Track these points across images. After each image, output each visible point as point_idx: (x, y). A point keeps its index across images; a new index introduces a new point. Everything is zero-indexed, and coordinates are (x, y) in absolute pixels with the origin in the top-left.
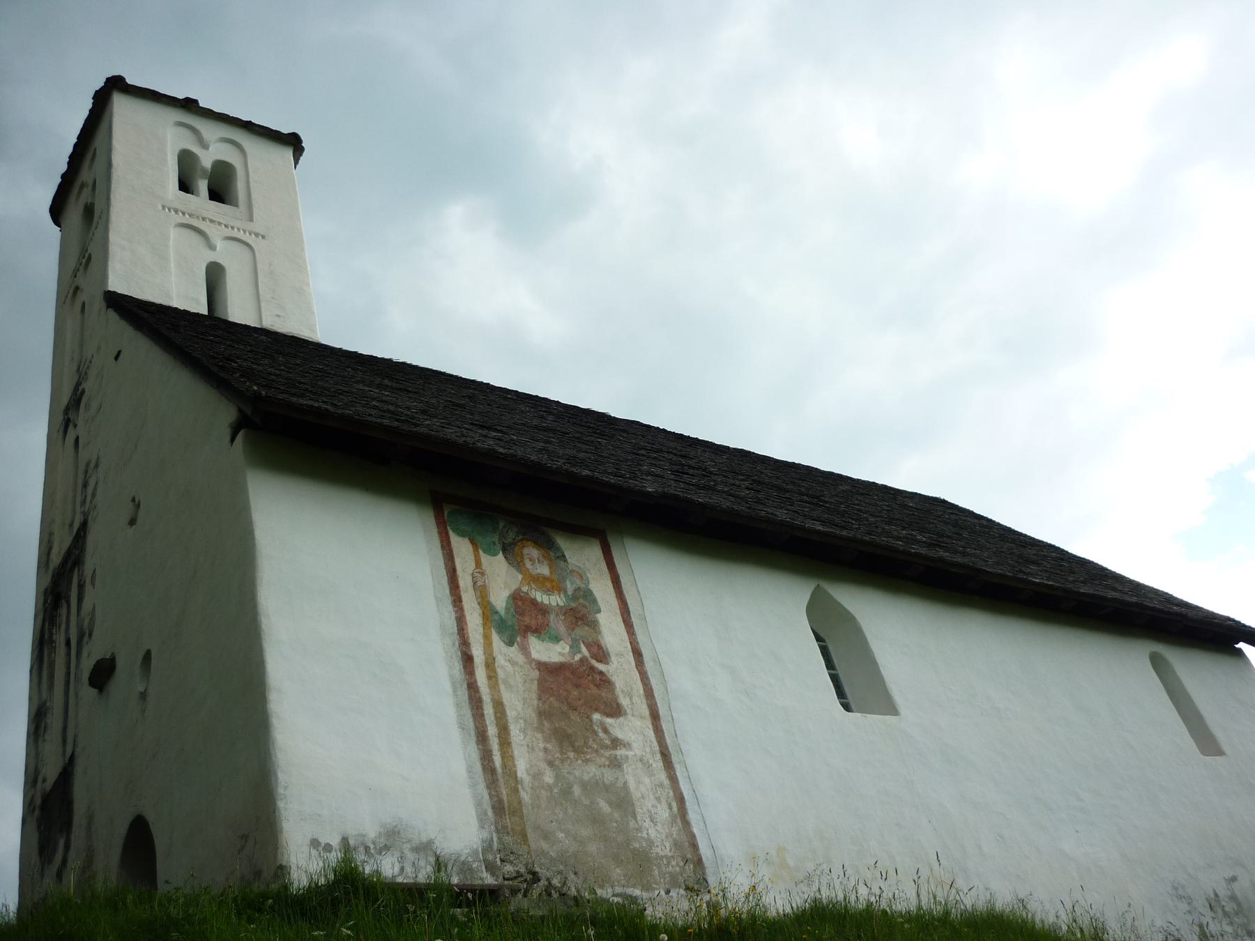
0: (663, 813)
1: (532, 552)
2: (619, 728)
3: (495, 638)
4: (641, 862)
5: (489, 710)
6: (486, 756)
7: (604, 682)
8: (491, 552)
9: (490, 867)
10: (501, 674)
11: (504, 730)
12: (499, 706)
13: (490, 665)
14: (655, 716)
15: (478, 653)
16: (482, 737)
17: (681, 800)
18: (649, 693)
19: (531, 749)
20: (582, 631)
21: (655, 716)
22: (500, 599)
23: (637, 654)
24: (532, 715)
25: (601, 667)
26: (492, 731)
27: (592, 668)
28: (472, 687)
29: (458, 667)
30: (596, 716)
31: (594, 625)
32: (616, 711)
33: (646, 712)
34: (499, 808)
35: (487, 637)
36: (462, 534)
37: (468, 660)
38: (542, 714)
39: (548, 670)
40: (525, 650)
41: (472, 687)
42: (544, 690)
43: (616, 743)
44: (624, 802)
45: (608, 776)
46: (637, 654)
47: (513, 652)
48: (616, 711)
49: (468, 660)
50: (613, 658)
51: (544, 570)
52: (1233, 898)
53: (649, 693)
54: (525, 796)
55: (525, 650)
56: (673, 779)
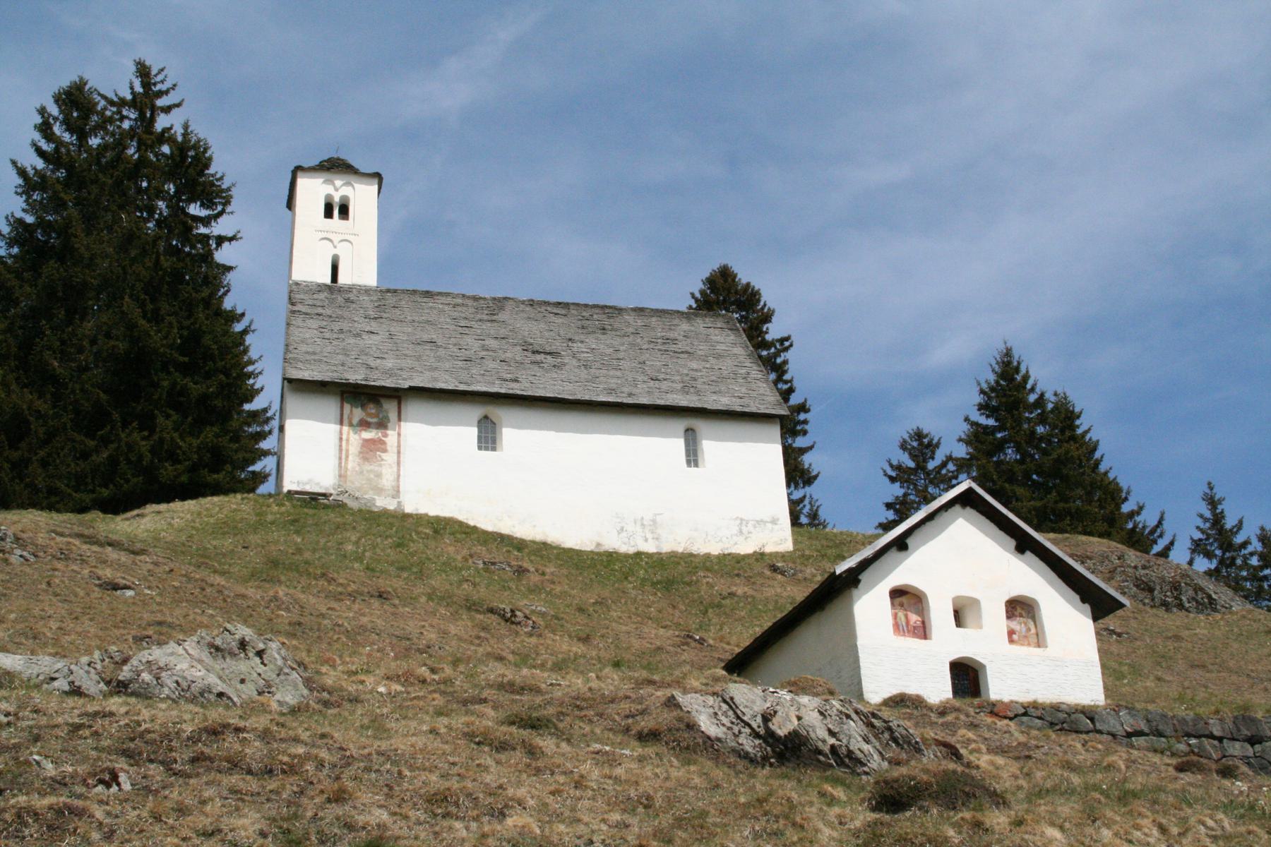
0: (392, 478)
1: (372, 406)
3: (351, 432)
4: (380, 491)
5: (344, 452)
6: (340, 464)
7: (384, 443)
8: (357, 407)
9: (334, 489)
11: (347, 457)
12: (347, 451)
13: (348, 440)
14: (399, 452)
15: (344, 437)
16: (340, 458)
17: (399, 476)
18: (399, 446)
21: (399, 452)
24: (357, 452)
26: (344, 456)
28: (341, 446)
29: (337, 441)
32: (385, 451)
34: (340, 476)
35: (348, 434)
37: (341, 439)
38: (360, 453)
39: (366, 441)
40: (360, 435)
41: (341, 446)
42: (363, 446)
44: (379, 475)
45: (376, 468)
47: (356, 437)
48: (385, 451)
51: (373, 411)
52: (654, 521)
53: (399, 446)
54: (349, 473)
55: (360, 435)
56: (399, 470)
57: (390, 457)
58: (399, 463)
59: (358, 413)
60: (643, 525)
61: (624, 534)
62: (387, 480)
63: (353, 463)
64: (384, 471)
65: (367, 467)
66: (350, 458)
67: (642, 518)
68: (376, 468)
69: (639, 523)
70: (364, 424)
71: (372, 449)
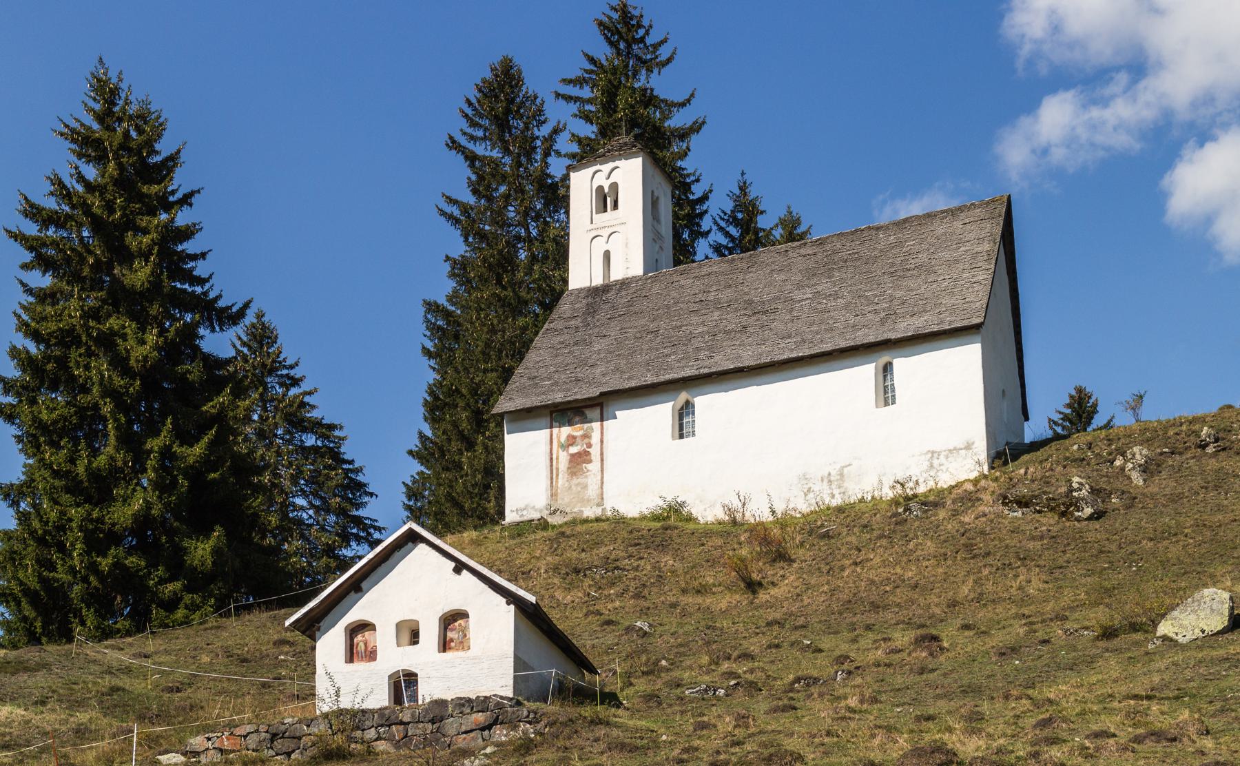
2: (589, 466)
6: (552, 483)
8: (564, 425)
10: (560, 460)
11: (557, 475)
12: (557, 469)
13: (557, 459)
14: (602, 460)
15: (554, 457)
16: (552, 478)
18: (602, 454)
19: (563, 478)
20: (586, 440)
21: (602, 460)
22: (563, 439)
23: (602, 442)
24: (565, 469)
25: (588, 450)
26: (554, 476)
27: (586, 451)
28: (552, 466)
29: (548, 461)
30: (584, 465)
32: (590, 461)
33: (599, 459)
35: (558, 451)
36: (556, 422)
37: (551, 459)
38: (568, 468)
39: (572, 456)
40: (567, 451)
41: (552, 466)
42: (570, 461)
43: (588, 471)
46: (602, 442)
47: (565, 453)
49: (551, 459)
50: (593, 447)
53: (602, 454)
57: (594, 467)
59: (566, 431)
60: (830, 481)
66: (560, 476)
67: (829, 474)
69: (826, 481)
71: (579, 460)
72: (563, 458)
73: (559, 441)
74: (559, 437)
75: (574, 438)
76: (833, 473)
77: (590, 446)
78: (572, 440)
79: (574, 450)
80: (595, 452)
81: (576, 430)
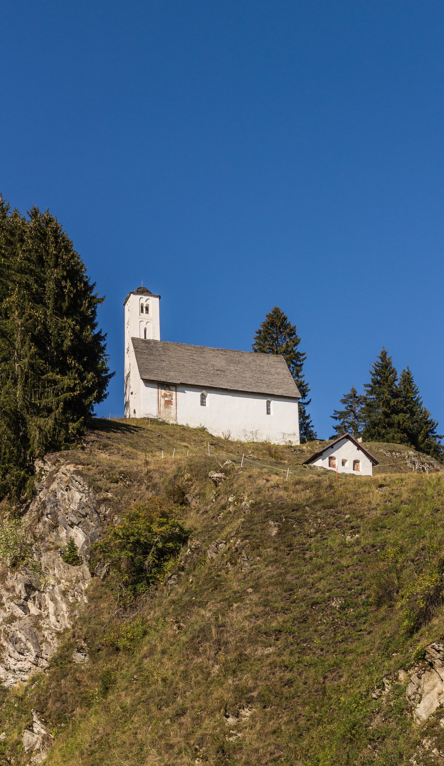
1: (167, 389)
2: (172, 406)
7: (172, 402)
8: (163, 389)
14: (176, 405)
15: (159, 399)
18: (176, 403)
20: (171, 397)
21: (176, 405)
22: (163, 394)
23: (176, 399)
31: (172, 396)
32: (172, 405)
37: (158, 400)
39: (166, 401)
42: (165, 403)
44: (170, 413)
45: (170, 410)
46: (176, 399)
48: (172, 405)
49: (158, 400)
52: (256, 433)
53: (176, 403)
57: (173, 407)
58: (176, 409)
59: (163, 392)
61: (246, 437)
62: (173, 414)
63: (162, 408)
64: (172, 412)
65: (167, 410)
68: (170, 410)
70: (165, 396)
71: (168, 403)
72: (162, 401)
73: (161, 395)
74: (161, 393)
75: (167, 395)
76: (254, 431)
77: (172, 399)
78: (165, 396)
79: (166, 399)
80: (174, 401)
81: (167, 392)
